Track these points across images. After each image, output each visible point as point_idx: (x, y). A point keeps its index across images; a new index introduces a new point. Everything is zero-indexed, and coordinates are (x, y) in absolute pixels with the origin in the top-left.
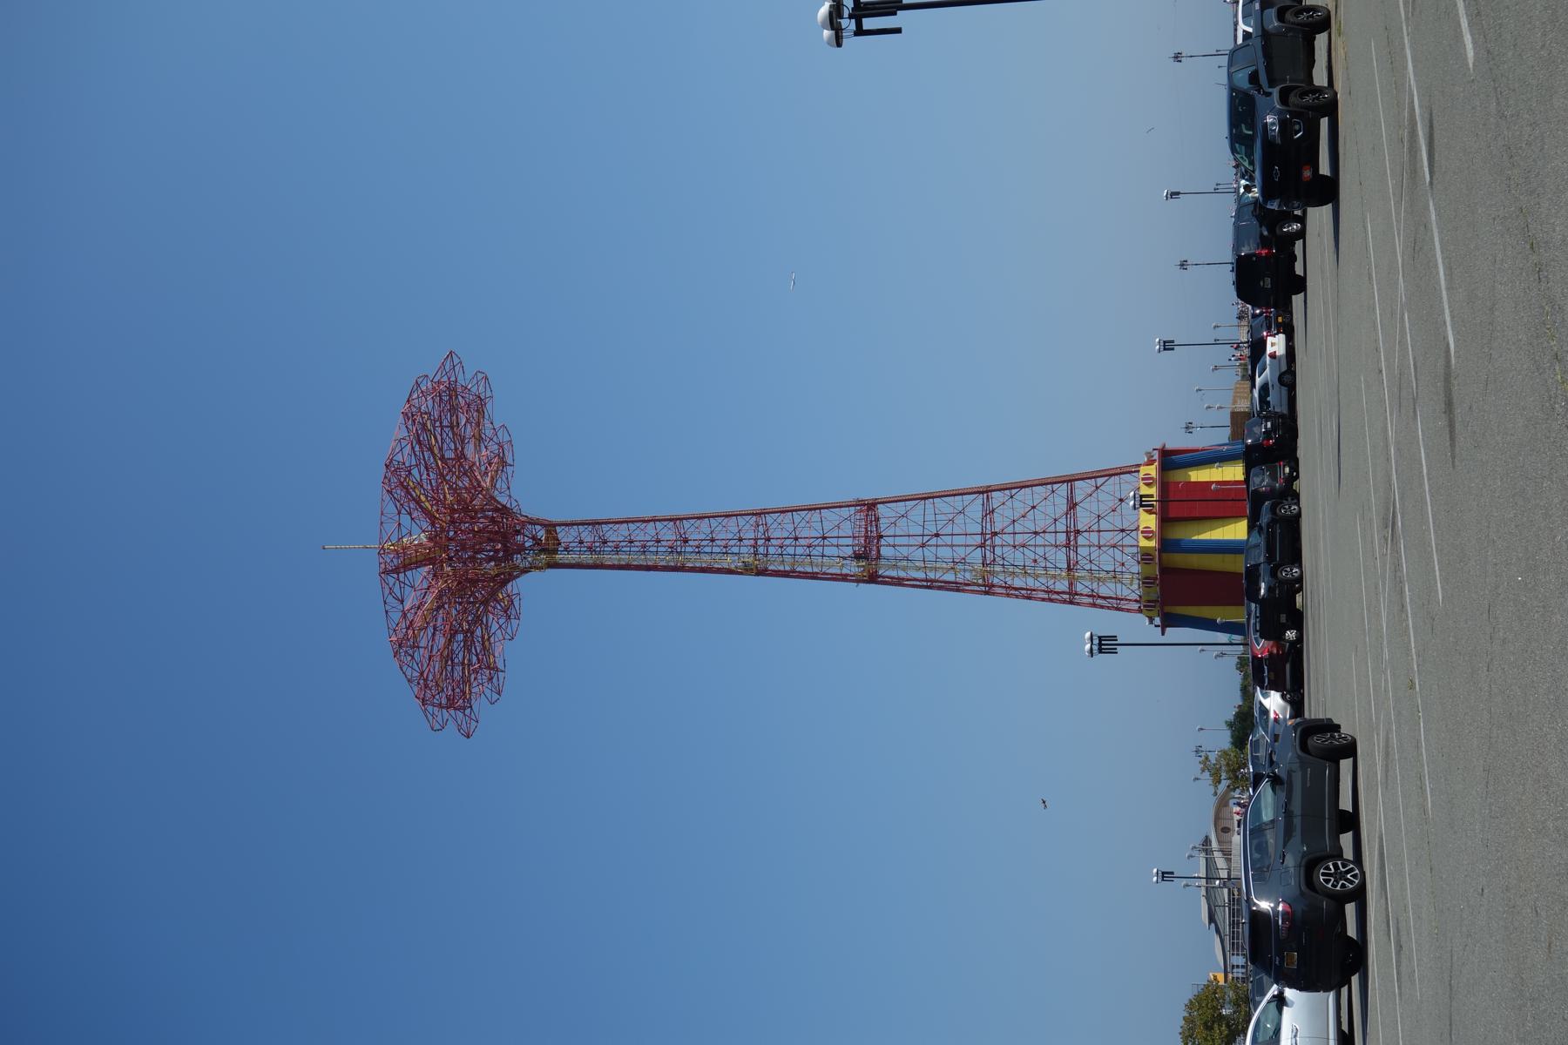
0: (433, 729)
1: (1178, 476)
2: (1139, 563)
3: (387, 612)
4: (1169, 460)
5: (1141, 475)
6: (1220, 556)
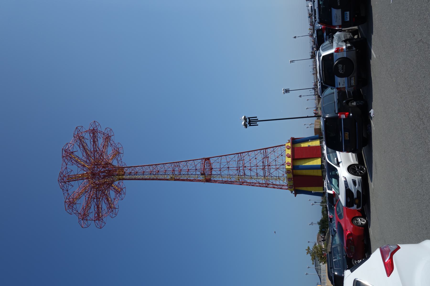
0: (83, 227)
1: (298, 145)
2: (286, 174)
3: (64, 194)
4: (294, 141)
5: (286, 146)
6: (312, 171)
